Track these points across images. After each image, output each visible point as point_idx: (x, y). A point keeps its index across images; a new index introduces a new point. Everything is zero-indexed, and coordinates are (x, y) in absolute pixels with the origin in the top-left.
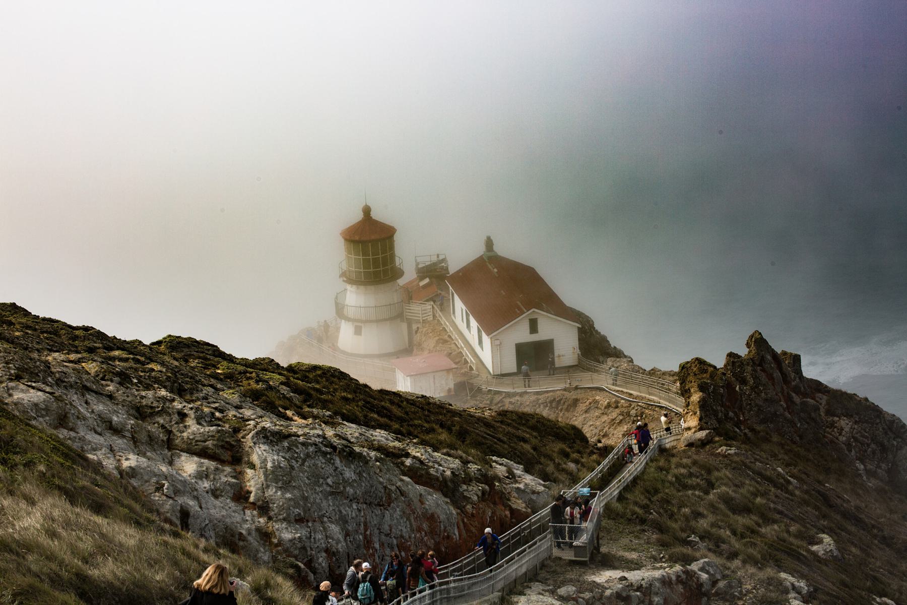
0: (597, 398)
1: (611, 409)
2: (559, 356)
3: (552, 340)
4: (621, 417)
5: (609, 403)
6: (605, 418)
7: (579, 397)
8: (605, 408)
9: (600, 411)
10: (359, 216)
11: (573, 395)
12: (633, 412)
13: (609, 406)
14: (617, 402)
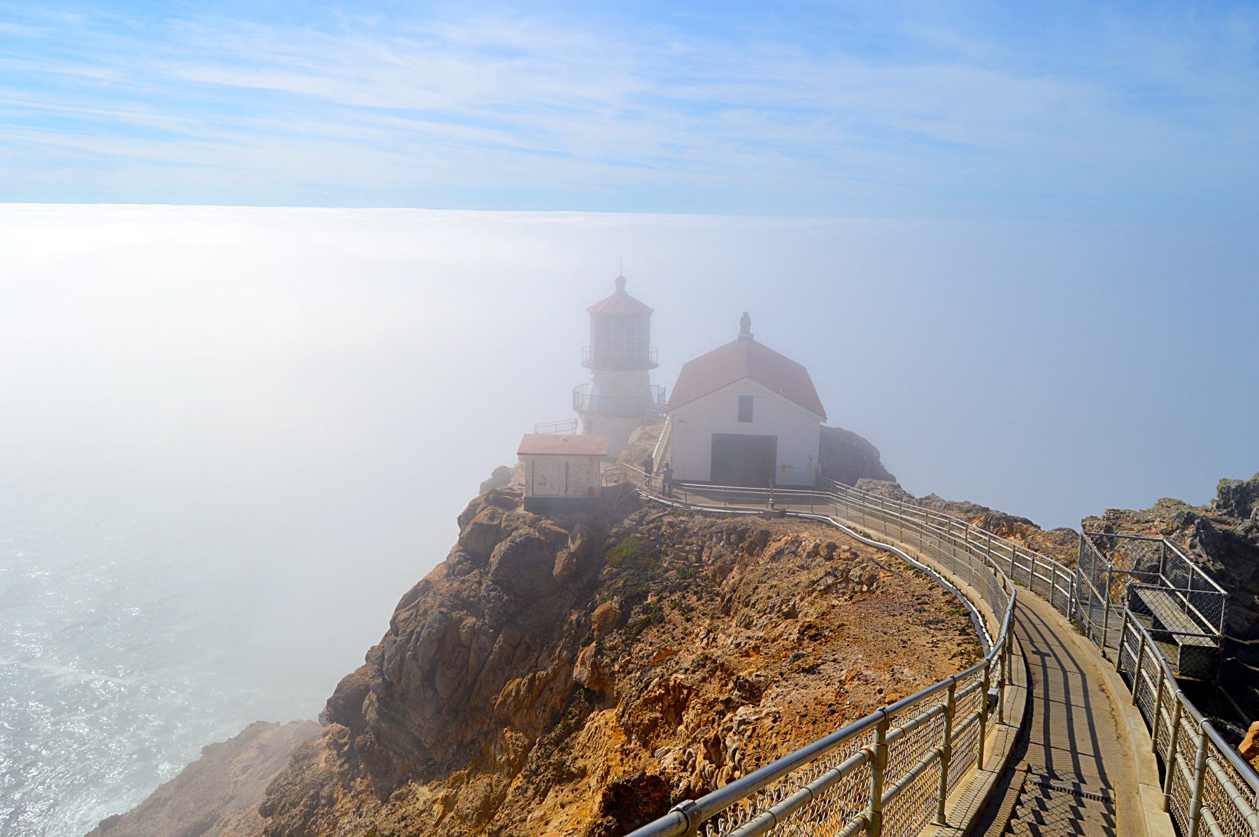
0: (805, 535)
1: (819, 560)
2: (784, 467)
3: (776, 437)
4: (830, 580)
5: (817, 547)
6: (804, 577)
7: (772, 530)
8: (809, 555)
9: (799, 561)
10: (611, 290)
11: (763, 524)
12: (855, 572)
13: (814, 553)
14: (832, 547)
